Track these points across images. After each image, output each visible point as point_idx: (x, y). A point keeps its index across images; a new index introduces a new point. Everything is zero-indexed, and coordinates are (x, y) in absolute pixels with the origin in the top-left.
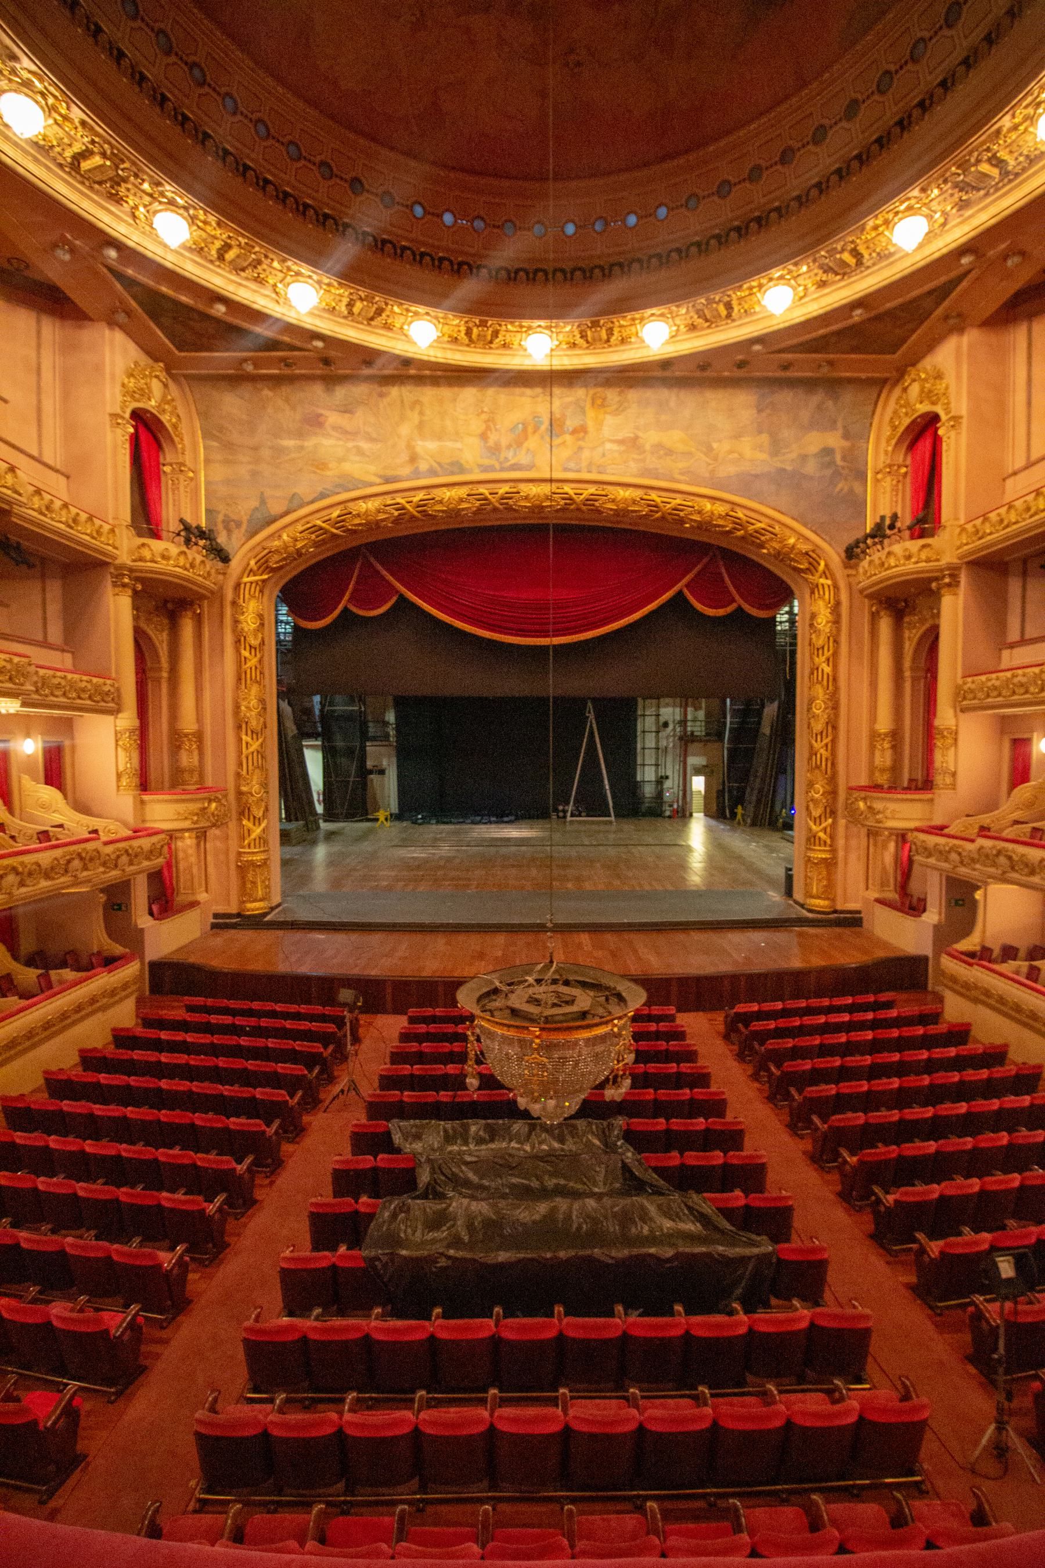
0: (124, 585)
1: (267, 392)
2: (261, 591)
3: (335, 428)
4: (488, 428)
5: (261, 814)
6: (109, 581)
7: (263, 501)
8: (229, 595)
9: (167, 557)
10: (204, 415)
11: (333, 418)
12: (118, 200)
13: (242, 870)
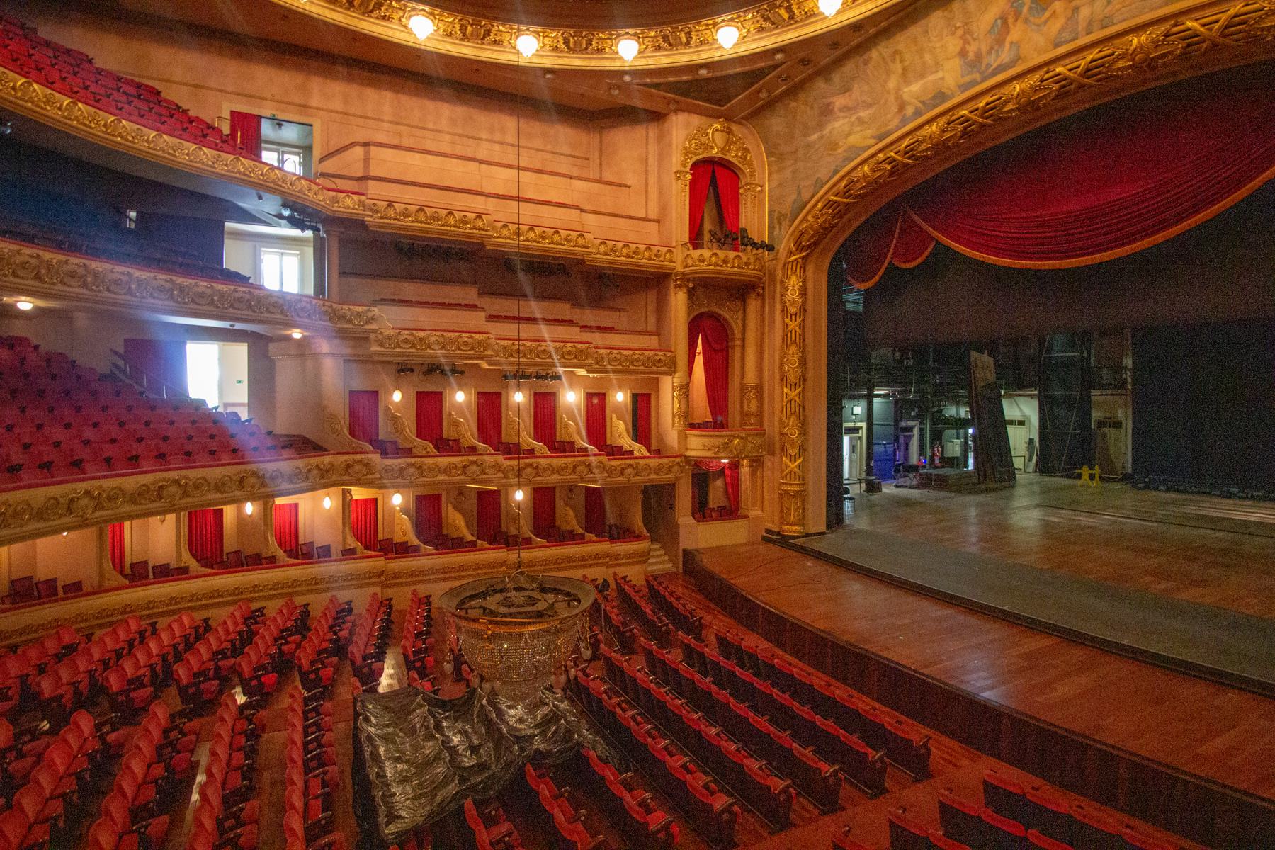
0: (680, 286)
1: (793, 104)
2: (804, 268)
3: (841, 110)
4: (966, 42)
5: (796, 451)
6: (672, 284)
7: (799, 193)
8: (779, 274)
9: (709, 259)
10: (765, 141)
11: (839, 102)
12: (600, 51)
13: (781, 496)
